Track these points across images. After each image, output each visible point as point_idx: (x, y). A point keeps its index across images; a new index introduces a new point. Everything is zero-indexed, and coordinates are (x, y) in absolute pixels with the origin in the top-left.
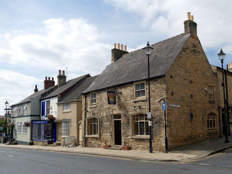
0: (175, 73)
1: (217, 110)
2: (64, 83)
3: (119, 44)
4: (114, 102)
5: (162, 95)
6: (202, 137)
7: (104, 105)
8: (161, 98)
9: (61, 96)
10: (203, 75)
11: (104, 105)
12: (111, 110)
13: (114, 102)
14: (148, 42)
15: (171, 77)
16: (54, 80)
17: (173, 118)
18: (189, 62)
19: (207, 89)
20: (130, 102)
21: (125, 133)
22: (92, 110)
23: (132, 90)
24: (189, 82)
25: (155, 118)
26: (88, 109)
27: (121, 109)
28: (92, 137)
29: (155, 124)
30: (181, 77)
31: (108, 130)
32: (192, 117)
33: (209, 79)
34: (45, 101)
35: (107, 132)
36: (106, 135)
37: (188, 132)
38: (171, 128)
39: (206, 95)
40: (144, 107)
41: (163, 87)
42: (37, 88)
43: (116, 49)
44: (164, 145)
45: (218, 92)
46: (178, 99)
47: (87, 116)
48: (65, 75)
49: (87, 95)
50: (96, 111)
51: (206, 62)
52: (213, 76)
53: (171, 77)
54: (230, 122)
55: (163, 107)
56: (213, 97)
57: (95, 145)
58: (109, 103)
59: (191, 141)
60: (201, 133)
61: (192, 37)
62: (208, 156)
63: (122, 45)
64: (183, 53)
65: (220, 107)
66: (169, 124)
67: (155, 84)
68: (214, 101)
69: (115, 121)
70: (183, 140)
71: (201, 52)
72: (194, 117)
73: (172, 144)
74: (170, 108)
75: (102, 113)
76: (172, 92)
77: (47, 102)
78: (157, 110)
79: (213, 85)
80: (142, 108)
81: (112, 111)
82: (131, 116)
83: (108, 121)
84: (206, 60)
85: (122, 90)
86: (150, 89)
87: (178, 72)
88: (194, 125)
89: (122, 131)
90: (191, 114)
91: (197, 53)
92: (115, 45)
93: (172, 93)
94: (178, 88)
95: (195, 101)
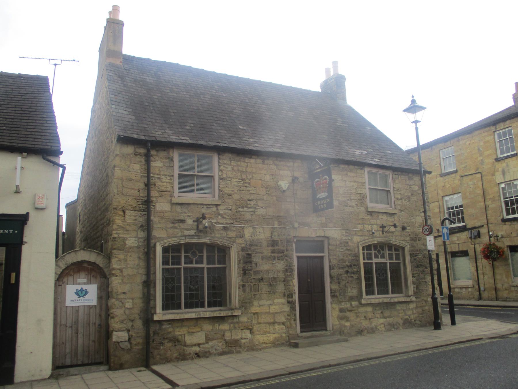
7: (260, 203)
11: (260, 203)
14: (413, 97)
25: (416, 256)
29: (417, 269)
31: (280, 288)
36: (269, 302)
49: (153, 152)
50: (220, 219)
75: (248, 232)
80: (386, 229)
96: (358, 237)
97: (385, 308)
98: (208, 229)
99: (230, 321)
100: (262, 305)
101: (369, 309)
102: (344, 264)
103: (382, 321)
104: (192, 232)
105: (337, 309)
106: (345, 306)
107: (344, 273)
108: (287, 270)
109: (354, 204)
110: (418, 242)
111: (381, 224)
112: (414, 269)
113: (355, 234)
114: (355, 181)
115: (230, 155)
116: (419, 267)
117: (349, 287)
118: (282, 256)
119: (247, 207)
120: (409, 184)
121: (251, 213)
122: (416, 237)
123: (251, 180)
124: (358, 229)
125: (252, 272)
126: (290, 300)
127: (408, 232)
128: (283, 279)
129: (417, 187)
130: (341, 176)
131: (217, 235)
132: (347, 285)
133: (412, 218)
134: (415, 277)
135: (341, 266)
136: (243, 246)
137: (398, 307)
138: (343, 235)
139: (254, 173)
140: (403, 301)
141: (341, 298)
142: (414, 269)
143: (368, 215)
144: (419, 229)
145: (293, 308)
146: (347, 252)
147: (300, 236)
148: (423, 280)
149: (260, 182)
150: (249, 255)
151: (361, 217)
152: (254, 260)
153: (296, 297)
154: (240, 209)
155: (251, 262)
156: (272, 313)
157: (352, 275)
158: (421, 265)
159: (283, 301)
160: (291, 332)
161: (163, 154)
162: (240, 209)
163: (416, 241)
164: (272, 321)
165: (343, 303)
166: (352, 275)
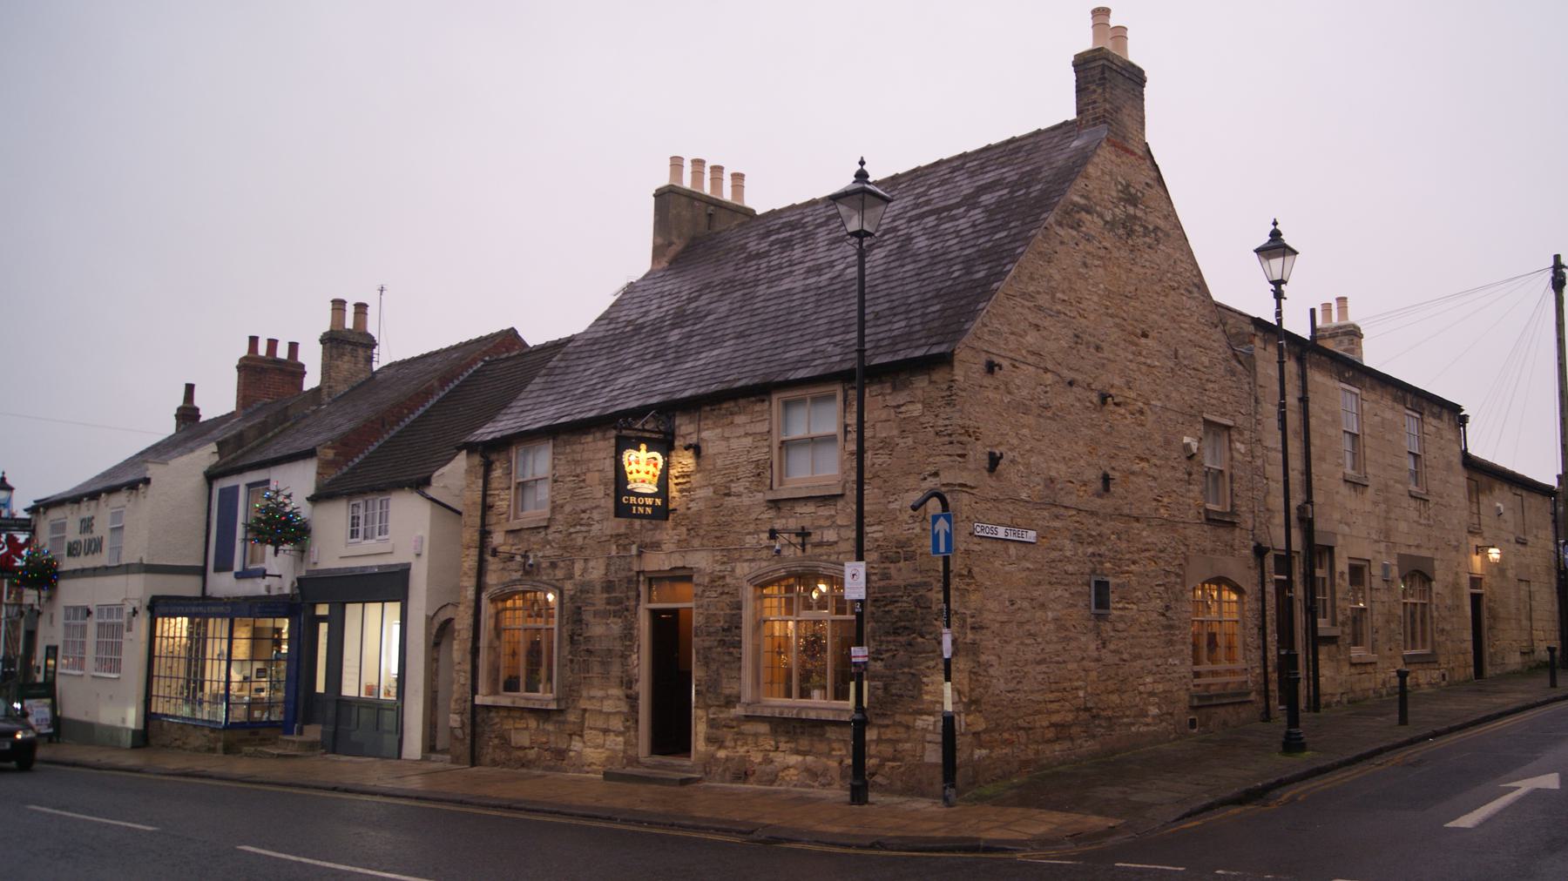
0: (1012, 346)
1: (1252, 563)
2: (363, 376)
3: (698, 163)
4: (658, 502)
5: (931, 469)
6: (1160, 718)
7: (596, 516)
8: (931, 483)
9: (336, 454)
10: (1171, 364)
11: (596, 516)
12: (634, 550)
13: (658, 502)
15: (991, 367)
16: (301, 358)
17: (992, 605)
18: (1096, 285)
19: (1194, 446)
20: (746, 501)
21: (712, 686)
22: (523, 546)
23: (761, 434)
24: (1095, 398)
26: (497, 539)
27: (696, 543)
28: (521, 704)
29: (890, 639)
30: (1046, 370)
31: (616, 670)
32: (1102, 600)
33: (1210, 386)
34: (241, 481)
35: (606, 676)
36: (600, 693)
37: (1076, 684)
38: (983, 658)
39: (1190, 474)
40: (830, 536)
41: (941, 422)
42: (197, 403)
43: (684, 190)
44: (934, 755)
45: (1259, 462)
46: (1024, 496)
47: (492, 579)
48: (372, 329)
49: (493, 457)
51: (1195, 290)
52: (1233, 373)
53: (991, 367)
54: (1321, 633)
55: (936, 538)
56: (1228, 492)
57: (532, 754)
58: (622, 510)
59: (1094, 737)
60: (1152, 694)
61: (1114, 145)
62: (1178, 820)
63: (718, 170)
64: (1062, 233)
65: (1267, 550)
66: (970, 636)
67: (899, 406)
68: (1233, 513)
69: (655, 614)
70: (1050, 734)
71: (1167, 235)
72: (1113, 597)
73: (984, 752)
74: (977, 548)
75: (578, 566)
76: (991, 454)
77: (250, 486)
78: (900, 551)
79: (1230, 423)
80: (815, 538)
81: (640, 554)
82: (751, 589)
83: (616, 614)
84: (1196, 280)
85: (705, 434)
86: (868, 433)
87: (1031, 338)
88: (1112, 647)
89: (697, 673)
90: (1097, 583)
91: (1145, 236)
92: (676, 163)
93: (994, 461)
94: (1025, 431)
95: (1126, 511)
96: (746, 564)
97: (799, 731)
98: (534, 569)
99: (555, 718)
100: (593, 697)
101: (763, 728)
102: (717, 625)
103: (794, 759)
104: (517, 576)
105: (704, 719)
106: (721, 716)
107: (716, 644)
108: (626, 636)
109: (742, 489)
110: (902, 564)
111: (799, 526)
112: (883, 638)
113: (741, 556)
114: (747, 434)
115: (565, 437)
116: (899, 634)
117: (724, 675)
118: (619, 611)
119: (581, 525)
120: (894, 404)
121: (585, 534)
122: (899, 550)
123: (588, 474)
124: (747, 546)
125: (581, 638)
126: (629, 692)
127: (876, 540)
128: (620, 654)
129: (920, 406)
130: (720, 430)
131: (545, 578)
132: (721, 671)
133: (891, 498)
134: (882, 660)
135: (712, 629)
136: (572, 593)
137: (831, 733)
138: (717, 562)
139: (590, 460)
140: (831, 718)
141: (710, 698)
142: (883, 638)
143: (771, 508)
144: (911, 526)
145: (634, 708)
146: (724, 596)
147: (646, 569)
148: (906, 670)
149: (597, 473)
150: (580, 608)
151: (754, 516)
152: (584, 617)
153: (643, 688)
154: (572, 530)
155: (581, 621)
156: (605, 713)
157: (731, 650)
158: (905, 628)
159: (616, 692)
160: (630, 752)
161: (503, 456)
162: (572, 530)
163: (899, 562)
164: (605, 726)
165: (713, 710)
166: (731, 650)
